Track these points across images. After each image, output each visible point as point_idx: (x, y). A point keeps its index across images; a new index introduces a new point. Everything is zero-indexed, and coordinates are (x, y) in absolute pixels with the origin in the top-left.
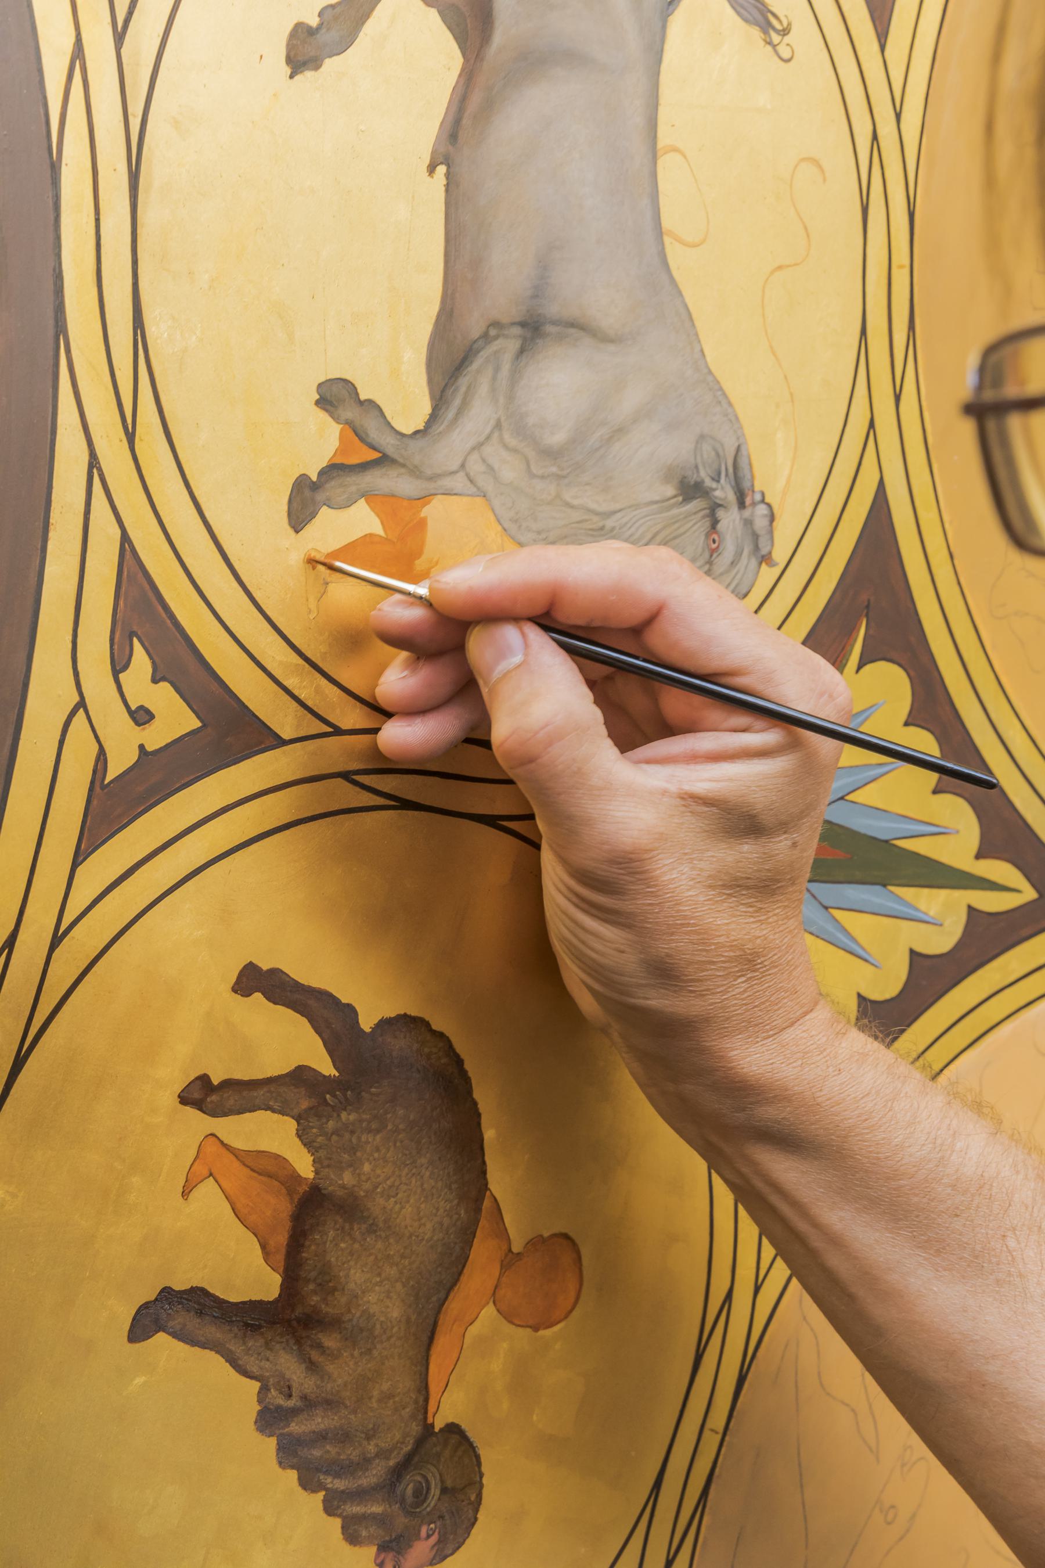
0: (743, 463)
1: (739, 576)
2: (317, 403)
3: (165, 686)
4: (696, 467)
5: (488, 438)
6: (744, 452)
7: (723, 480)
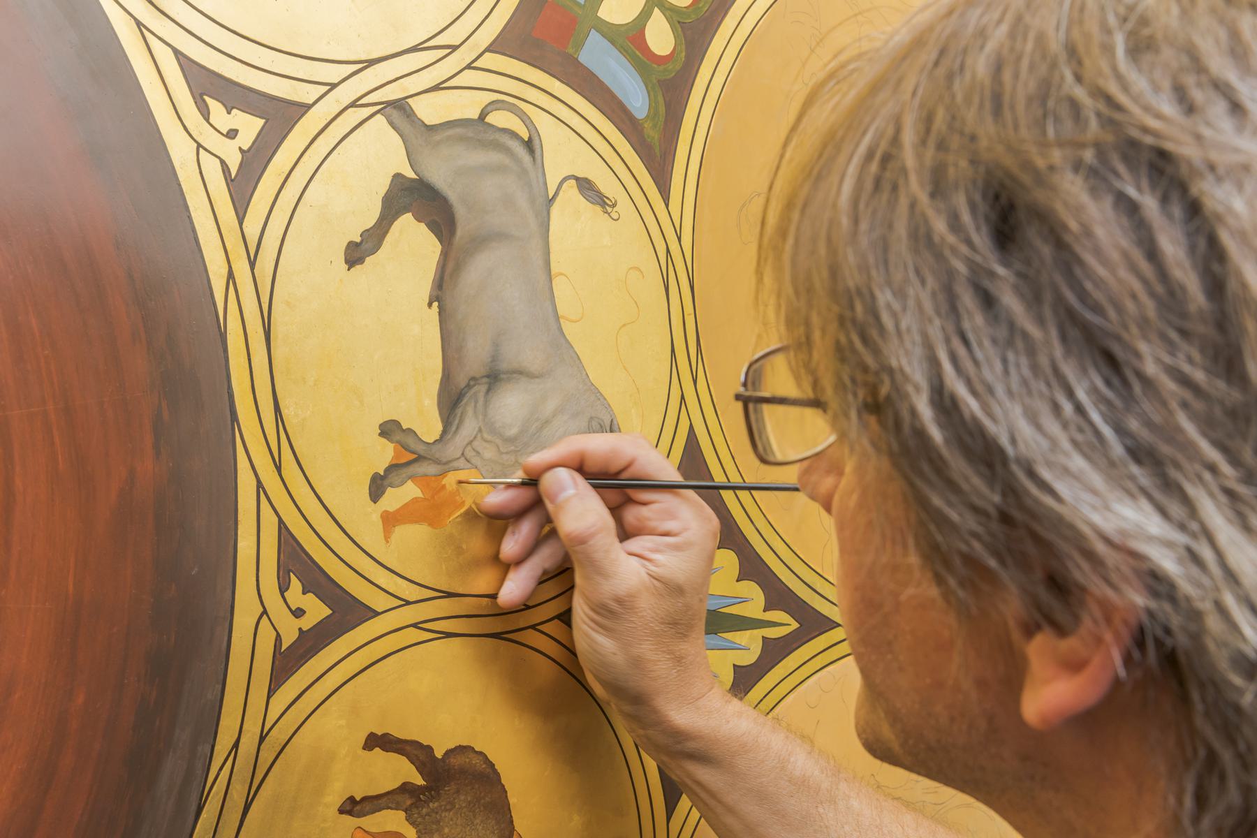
3: (310, 595)
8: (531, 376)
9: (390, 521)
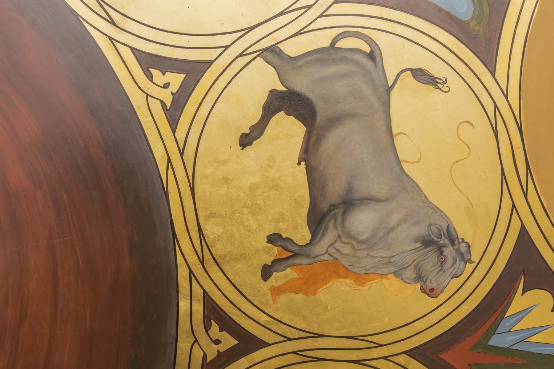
0: (452, 230)
1: (456, 269)
2: (267, 242)
3: (224, 333)
4: (430, 235)
5: (336, 241)
6: (451, 226)
7: (443, 238)
8: (378, 200)
9: (276, 291)
